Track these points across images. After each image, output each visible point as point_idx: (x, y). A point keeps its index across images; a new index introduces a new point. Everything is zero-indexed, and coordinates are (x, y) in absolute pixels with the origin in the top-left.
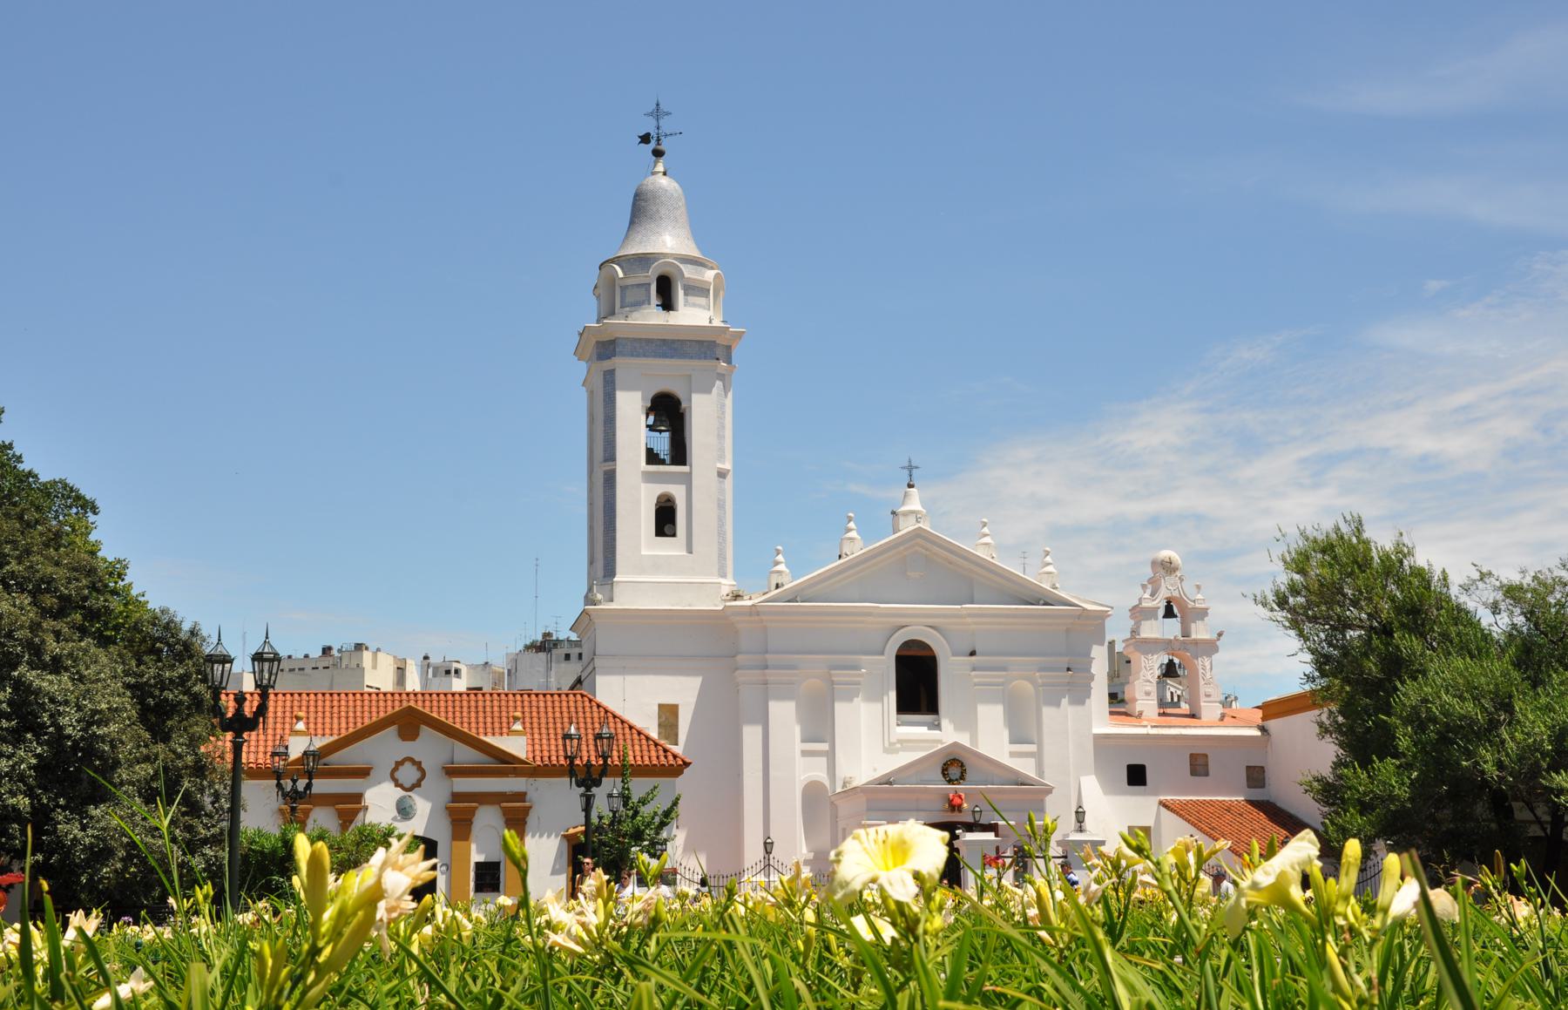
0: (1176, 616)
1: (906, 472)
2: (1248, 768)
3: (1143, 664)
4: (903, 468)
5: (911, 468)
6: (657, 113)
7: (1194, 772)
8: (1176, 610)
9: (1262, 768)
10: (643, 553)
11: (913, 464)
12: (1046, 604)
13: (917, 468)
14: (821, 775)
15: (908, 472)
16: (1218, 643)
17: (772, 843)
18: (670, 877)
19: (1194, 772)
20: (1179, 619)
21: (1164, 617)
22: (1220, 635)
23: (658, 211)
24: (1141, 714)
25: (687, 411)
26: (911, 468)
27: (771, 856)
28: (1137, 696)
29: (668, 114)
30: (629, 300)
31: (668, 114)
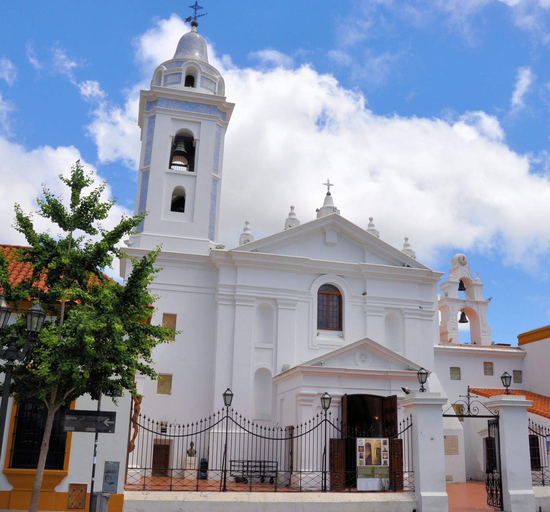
1: (326, 187)
2: (514, 371)
3: (451, 313)
4: (325, 184)
5: (329, 185)
6: (196, 7)
7: (486, 373)
9: (520, 371)
11: (330, 183)
12: (408, 266)
14: (267, 365)
15: (327, 187)
16: (488, 304)
17: (232, 395)
18: (107, 422)
19: (486, 373)
22: (490, 299)
23: (191, 45)
24: (451, 341)
25: (197, 142)
26: (329, 185)
28: (449, 331)
29: (201, 8)
31: (201, 8)
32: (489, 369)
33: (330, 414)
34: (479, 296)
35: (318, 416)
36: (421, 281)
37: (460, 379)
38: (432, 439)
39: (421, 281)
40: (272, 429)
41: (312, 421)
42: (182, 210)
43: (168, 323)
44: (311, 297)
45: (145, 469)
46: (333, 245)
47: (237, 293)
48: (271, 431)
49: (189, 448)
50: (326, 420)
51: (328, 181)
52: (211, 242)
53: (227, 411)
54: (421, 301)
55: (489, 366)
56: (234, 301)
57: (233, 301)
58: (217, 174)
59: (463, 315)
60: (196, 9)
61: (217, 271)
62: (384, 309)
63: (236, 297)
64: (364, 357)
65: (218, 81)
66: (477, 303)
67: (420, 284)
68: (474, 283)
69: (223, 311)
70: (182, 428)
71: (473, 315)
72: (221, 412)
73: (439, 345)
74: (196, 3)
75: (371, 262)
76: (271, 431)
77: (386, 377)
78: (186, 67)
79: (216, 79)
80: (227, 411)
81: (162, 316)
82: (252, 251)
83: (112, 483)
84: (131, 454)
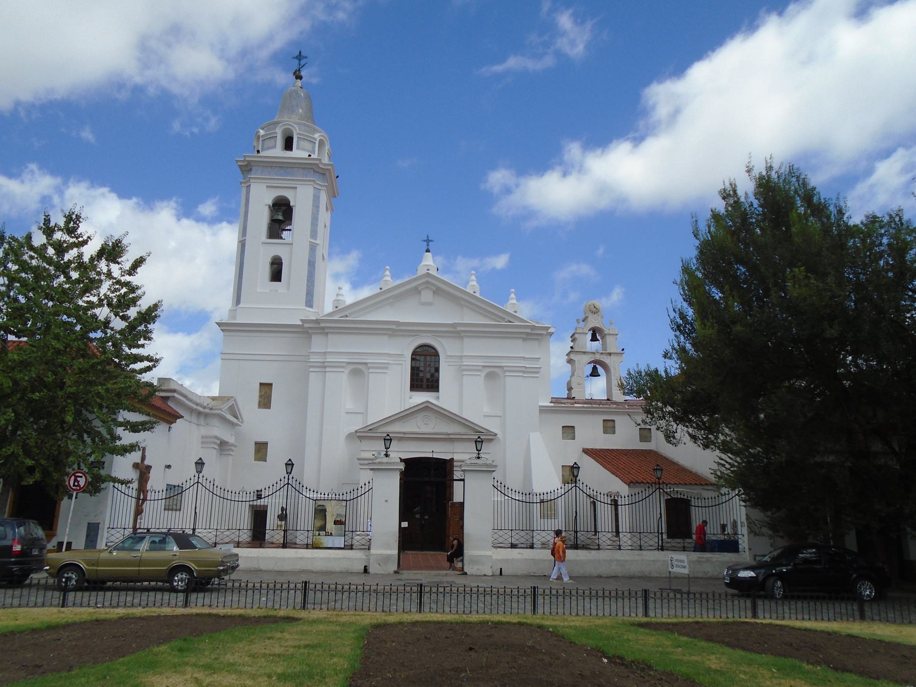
0: (598, 340)
1: (426, 243)
5: (428, 241)
6: (300, 57)
8: (599, 337)
10: (258, 290)
11: (430, 239)
12: (511, 322)
13: (431, 241)
20: (601, 342)
21: (591, 340)
26: (428, 241)
27: (201, 475)
30: (265, 147)
31: (306, 57)
32: (609, 427)
33: (293, 478)
34: (613, 345)
35: (281, 480)
36: (525, 336)
37: (574, 439)
38: (386, 501)
39: (525, 336)
40: (237, 492)
41: (275, 485)
42: (280, 280)
43: (266, 392)
44: (403, 359)
45: (125, 528)
46: (430, 304)
47: (328, 360)
48: (237, 494)
49: (280, 512)
50: (288, 484)
51: (428, 237)
52: (308, 309)
53: (199, 478)
54: (524, 358)
55: (610, 424)
56: (325, 367)
57: (323, 366)
58: (316, 239)
59: (595, 368)
60: (300, 60)
61: (311, 338)
62: (481, 368)
63: (326, 364)
64: (427, 420)
65: (318, 140)
66: (610, 354)
67: (524, 339)
68: (606, 333)
69: (314, 379)
70: (157, 493)
71: (605, 366)
72: (192, 478)
73: (551, 402)
74: (300, 52)
75: (471, 318)
76: (237, 494)
77: (449, 439)
78: (281, 130)
79: (316, 139)
80: (199, 478)
81: (258, 385)
82: (342, 317)
83: (93, 541)
84: (139, 517)
